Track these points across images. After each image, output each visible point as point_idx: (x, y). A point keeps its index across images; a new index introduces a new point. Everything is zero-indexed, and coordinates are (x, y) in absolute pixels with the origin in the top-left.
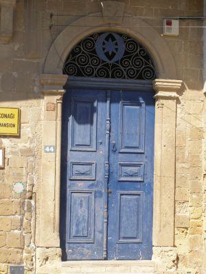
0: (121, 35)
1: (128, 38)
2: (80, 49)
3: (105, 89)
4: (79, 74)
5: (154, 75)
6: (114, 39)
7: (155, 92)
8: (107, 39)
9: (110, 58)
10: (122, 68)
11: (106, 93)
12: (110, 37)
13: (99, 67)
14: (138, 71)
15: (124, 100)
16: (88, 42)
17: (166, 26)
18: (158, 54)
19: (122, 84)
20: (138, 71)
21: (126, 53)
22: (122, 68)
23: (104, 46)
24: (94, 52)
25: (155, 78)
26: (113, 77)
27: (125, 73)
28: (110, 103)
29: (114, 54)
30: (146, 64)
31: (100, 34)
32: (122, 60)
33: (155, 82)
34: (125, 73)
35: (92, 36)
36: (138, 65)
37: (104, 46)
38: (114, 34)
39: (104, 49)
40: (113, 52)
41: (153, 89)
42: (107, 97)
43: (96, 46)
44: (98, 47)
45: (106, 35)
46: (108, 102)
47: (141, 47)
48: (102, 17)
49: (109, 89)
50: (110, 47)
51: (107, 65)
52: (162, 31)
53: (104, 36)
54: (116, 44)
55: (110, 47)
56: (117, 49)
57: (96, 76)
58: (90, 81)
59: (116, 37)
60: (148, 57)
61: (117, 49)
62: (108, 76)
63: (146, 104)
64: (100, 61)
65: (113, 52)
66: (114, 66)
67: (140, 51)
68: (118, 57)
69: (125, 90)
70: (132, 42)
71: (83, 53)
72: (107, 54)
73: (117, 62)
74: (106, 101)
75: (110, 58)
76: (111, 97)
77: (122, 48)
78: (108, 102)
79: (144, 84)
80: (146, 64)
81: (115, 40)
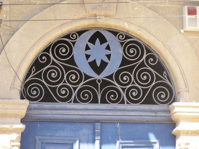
0: (115, 33)
1: (127, 37)
2: (48, 57)
3: (93, 122)
4: (48, 99)
5: (171, 97)
6: (103, 40)
7: (174, 124)
8: (92, 40)
9: (99, 69)
10: (119, 87)
11: (94, 129)
12: (98, 37)
13: (80, 86)
14: (145, 91)
15: (122, 139)
16: (61, 48)
17: (187, 17)
18: (176, 60)
19: (119, 113)
20: (145, 91)
21: (124, 62)
22: (119, 87)
23: (88, 52)
24: (72, 62)
25: (174, 101)
26: (103, 101)
27: (124, 95)
28: (101, 144)
29: (104, 64)
30: (158, 78)
31: (80, 33)
32: (118, 72)
33: (174, 107)
34: (124, 95)
35: (68, 36)
36: (126, 81)
37: (88, 52)
38: (103, 32)
39: (88, 56)
40: (102, 61)
41: (172, 121)
42: (94, 134)
43: (74, 52)
44: (78, 53)
45: (92, 33)
46: (97, 142)
47: (148, 51)
48: (83, 3)
49: (97, 121)
50: (98, 52)
51: (93, 83)
52: (181, 25)
53: (87, 36)
54: (108, 48)
55: (98, 52)
56: (109, 56)
57: (75, 101)
58: (124, 110)
59: (108, 35)
60: (160, 67)
61: (109, 56)
62: (95, 101)
63: (161, 145)
64: (82, 76)
65: (102, 61)
66: (104, 83)
67: (147, 58)
68: (113, 67)
69: (124, 123)
70: (131, 44)
71: (54, 63)
72: (93, 64)
73: (110, 77)
74: (94, 142)
75: (99, 69)
76: (101, 135)
77: (118, 53)
78: (97, 142)
79: (155, 112)
80: (158, 78)
81: (106, 41)
